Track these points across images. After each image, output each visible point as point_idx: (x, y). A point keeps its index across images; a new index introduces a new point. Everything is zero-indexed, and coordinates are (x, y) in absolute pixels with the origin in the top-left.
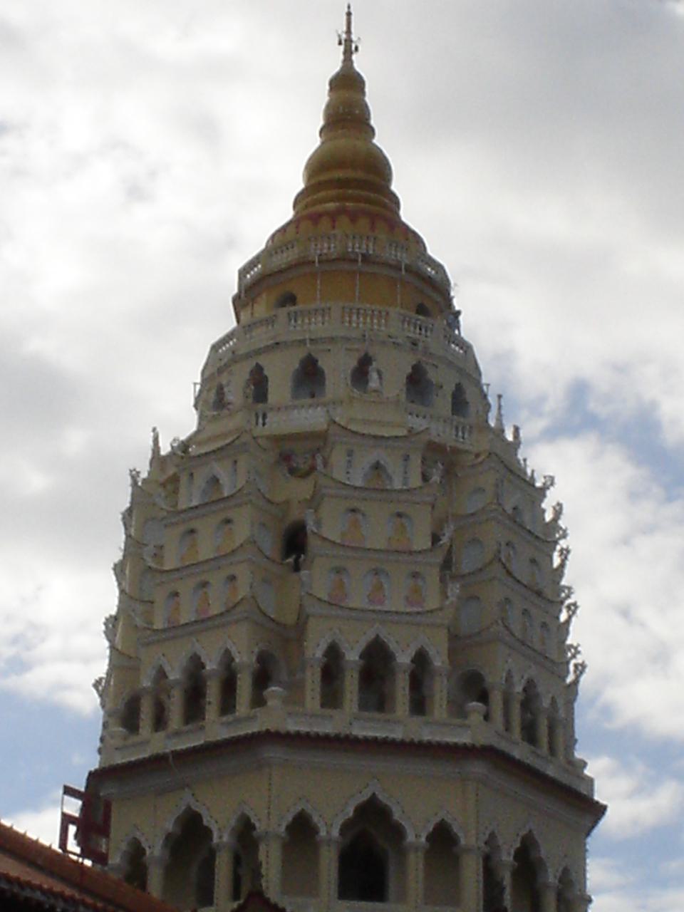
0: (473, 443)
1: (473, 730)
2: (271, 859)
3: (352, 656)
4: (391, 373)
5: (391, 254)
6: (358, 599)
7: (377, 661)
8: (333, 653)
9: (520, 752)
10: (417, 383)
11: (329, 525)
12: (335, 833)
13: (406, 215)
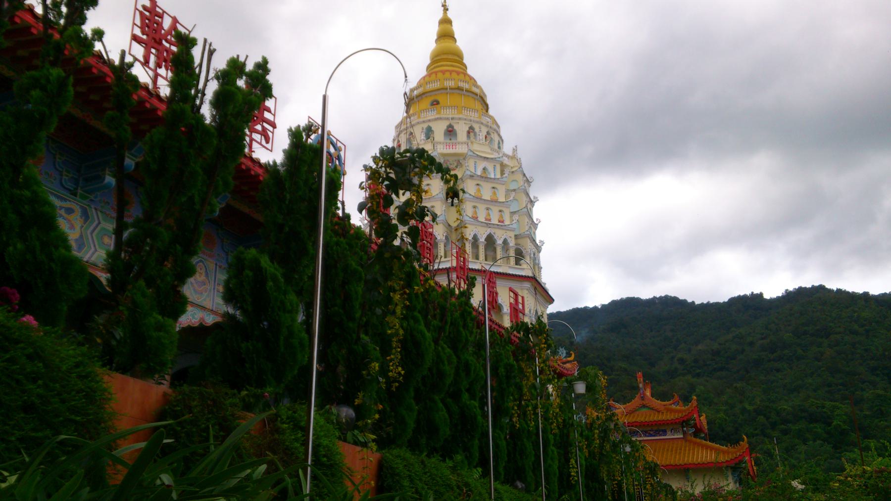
3: (482, 239)
6: (482, 219)
7: (490, 240)
8: (475, 238)
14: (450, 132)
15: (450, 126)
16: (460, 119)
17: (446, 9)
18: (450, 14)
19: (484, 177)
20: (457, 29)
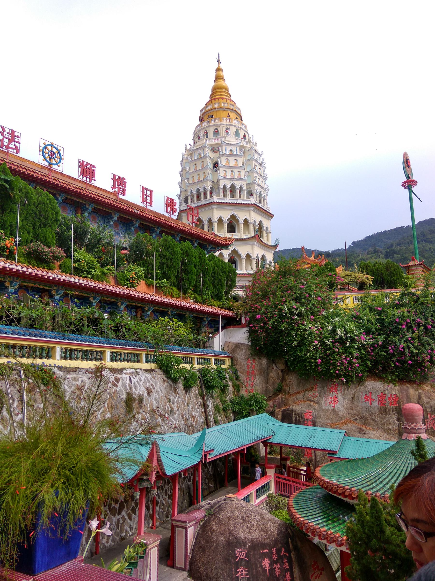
0: (247, 145)
1: (253, 200)
2: (215, 225)
3: (228, 187)
4: (232, 130)
5: (231, 107)
7: (233, 188)
8: (225, 187)
9: (260, 205)
10: (237, 134)
11: (223, 162)
12: (227, 221)
13: (232, 98)
14: (216, 132)
15: (216, 129)
16: (221, 124)
17: (219, 62)
18: (222, 66)
19: (231, 155)
20: (225, 74)
